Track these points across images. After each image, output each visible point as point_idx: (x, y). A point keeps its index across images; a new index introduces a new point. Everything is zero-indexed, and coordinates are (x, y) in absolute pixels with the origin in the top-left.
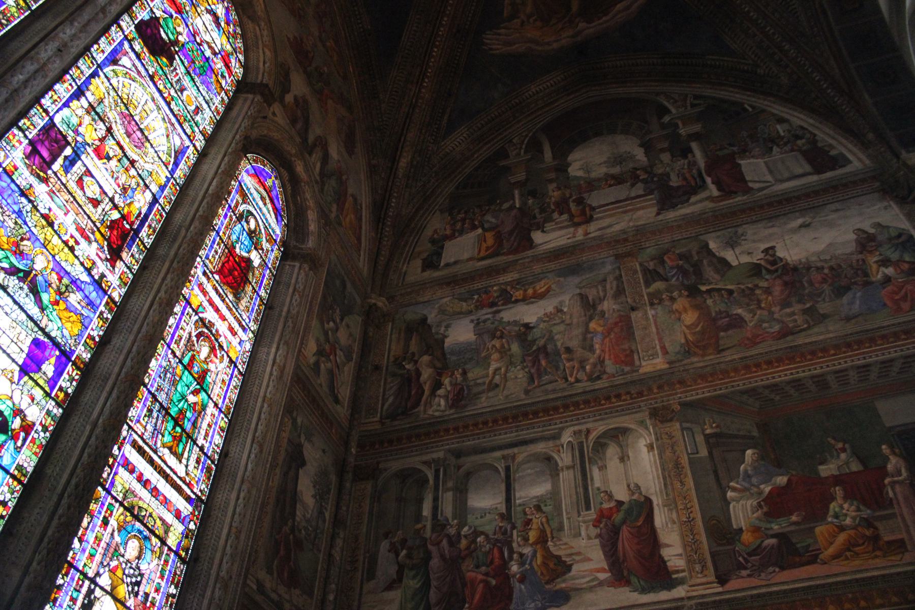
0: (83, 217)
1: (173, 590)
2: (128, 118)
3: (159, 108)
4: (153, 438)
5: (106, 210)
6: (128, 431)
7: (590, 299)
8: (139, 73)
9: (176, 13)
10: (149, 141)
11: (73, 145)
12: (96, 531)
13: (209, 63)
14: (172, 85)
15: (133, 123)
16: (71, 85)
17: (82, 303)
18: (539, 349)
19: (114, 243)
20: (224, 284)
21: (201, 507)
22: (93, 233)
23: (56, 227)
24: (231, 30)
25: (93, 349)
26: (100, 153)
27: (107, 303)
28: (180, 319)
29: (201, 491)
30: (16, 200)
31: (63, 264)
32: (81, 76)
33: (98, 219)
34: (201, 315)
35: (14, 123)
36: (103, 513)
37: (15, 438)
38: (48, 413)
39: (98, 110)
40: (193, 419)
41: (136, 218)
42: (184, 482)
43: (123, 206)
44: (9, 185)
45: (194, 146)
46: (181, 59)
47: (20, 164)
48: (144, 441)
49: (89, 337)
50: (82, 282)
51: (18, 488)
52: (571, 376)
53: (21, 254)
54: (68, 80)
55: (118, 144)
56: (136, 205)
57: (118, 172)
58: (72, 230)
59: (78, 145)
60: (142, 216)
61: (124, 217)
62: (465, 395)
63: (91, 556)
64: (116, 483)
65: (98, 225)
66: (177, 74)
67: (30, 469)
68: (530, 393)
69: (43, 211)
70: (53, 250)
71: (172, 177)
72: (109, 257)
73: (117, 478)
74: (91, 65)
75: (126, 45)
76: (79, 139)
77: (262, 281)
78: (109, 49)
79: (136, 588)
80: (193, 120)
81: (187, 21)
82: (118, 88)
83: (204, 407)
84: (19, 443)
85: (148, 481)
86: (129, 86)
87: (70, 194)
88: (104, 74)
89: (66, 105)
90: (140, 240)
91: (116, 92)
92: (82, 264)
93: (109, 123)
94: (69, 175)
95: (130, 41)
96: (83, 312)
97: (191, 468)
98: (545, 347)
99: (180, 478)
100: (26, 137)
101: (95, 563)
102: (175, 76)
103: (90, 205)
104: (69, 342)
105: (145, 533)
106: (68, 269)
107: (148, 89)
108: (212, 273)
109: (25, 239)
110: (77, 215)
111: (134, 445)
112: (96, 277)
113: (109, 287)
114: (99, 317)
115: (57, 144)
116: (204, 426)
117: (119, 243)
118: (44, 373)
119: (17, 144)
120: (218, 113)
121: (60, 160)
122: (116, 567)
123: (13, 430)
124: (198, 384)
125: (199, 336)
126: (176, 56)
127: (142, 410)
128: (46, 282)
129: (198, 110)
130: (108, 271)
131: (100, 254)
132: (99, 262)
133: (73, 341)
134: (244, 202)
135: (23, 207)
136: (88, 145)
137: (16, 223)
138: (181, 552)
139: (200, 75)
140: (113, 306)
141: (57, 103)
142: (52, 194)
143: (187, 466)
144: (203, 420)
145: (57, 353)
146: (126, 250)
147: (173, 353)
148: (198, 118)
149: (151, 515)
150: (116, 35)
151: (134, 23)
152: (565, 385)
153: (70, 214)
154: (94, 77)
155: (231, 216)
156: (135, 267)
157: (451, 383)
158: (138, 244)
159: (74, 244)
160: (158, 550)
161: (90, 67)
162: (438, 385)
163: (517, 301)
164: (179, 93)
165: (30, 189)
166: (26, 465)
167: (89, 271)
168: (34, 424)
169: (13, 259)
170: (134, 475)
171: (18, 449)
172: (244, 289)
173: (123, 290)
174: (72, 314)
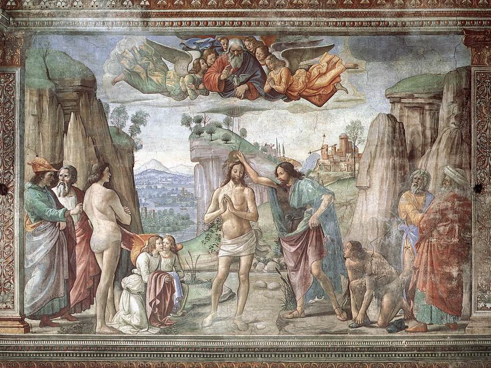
7: (408, 131)
18: (307, 231)
52: (358, 310)
62: (176, 302)
68: (289, 328)
98: (318, 229)
152: (344, 326)
157: (149, 264)
162: (124, 267)
163: (272, 95)
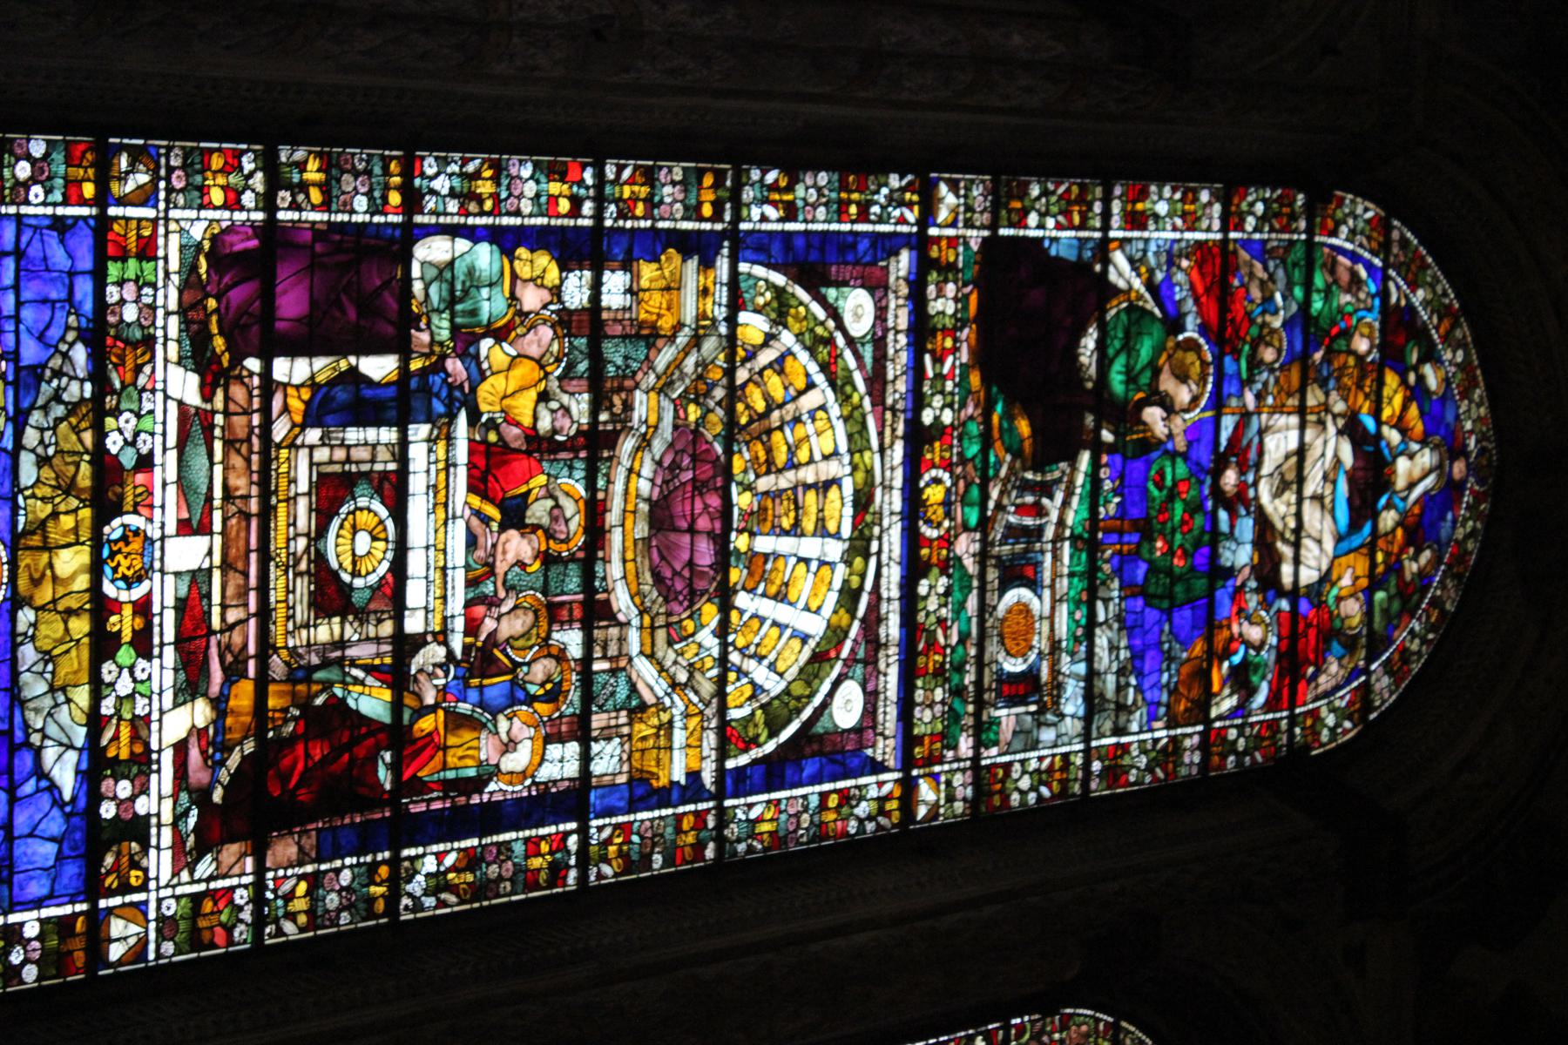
0: (243, 593)
2: (706, 471)
3: (860, 546)
5: (350, 652)
8: (877, 382)
9: (1203, 329)
10: (726, 607)
11: (416, 365)
13: (1212, 590)
14: (984, 524)
15: (715, 501)
19: (284, 778)
22: (234, 672)
23: (114, 529)
24: (1411, 568)
27: (65, 924)
30: (54, 333)
31: (28, 654)
32: (640, 209)
33: (293, 651)
39: (615, 354)
41: (448, 786)
43: (430, 699)
44: (72, 274)
45: (908, 787)
46: (1095, 481)
47: (171, 250)
50: (40, 772)
54: (581, 183)
55: (595, 510)
56: (487, 749)
57: (509, 588)
58: (165, 593)
59: (436, 380)
60: (475, 800)
61: (397, 734)
65: (277, 665)
66: (1039, 511)
69: (114, 443)
70: (36, 582)
72: (217, 796)
74: (707, 210)
75: (903, 263)
76: (455, 366)
80: (980, 704)
81: (1230, 388)
82: (751, 356)
86: (800, 383)
87: (266, 493)
88: (734, 274)
89: (507, 241)
90: (395, 862)
91: (731, 359)
92: (95, 722)
93: (614, 418)
94: (313, 435)
95: (924, 265)
100: (268, 203)
102: (1021, 509)
103: (302, 586)
106: (34, 687)
107: (872, 459)
110: (226, 566)
112: (108, 810)
113: (125, 888)
115: (359, 315)
117: (303, 796)
119: (217, 196)
120: (1114, 773)
121: (322, 366)
126: (1085, 459)
129: (1022, 688)
130: (167, 836)
131: (194, 754)
132: (164, 779)
135: (58, 374)
139: (1130, 589)
140: (80, 958)
141: (473, 207)
142: (196, 429)
146: (310, 842)
148: (1006, 717)
151: (994, 226)
153: (201, 542)
154: (686, 255)
156: (289, 927)
158: (375, 865)
159: (127, 635)
161: (693, 212)
164: (992, 575)
165: (135, 345)
167: (96, 767)
173: (168, 947)
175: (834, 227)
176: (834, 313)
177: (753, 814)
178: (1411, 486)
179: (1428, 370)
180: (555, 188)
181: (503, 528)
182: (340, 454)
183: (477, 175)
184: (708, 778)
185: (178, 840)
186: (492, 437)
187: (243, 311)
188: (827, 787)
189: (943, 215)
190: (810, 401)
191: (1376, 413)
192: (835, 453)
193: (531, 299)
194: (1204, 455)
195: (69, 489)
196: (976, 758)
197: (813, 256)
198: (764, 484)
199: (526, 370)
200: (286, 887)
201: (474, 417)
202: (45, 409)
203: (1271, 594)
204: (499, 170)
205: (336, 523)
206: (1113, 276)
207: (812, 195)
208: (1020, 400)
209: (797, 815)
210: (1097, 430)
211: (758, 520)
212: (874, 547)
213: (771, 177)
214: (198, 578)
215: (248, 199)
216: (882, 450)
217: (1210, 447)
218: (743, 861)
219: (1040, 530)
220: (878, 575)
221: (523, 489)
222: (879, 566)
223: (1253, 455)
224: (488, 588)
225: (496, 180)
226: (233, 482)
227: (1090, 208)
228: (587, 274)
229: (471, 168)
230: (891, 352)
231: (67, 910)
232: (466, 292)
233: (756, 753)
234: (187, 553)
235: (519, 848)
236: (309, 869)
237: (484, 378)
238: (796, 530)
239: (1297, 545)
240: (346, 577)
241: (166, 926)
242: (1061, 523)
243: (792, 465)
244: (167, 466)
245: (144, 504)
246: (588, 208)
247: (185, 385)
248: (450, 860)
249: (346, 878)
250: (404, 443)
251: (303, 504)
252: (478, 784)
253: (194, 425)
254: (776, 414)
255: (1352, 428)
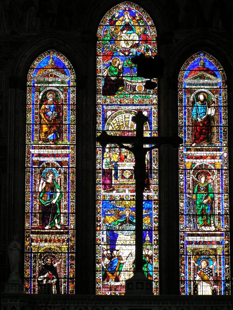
1: (227, 266)
4: (195, 228)
6: (184, 233)
8: (116, 110)
11: (113, 169)
12: (188, 268)
16: (100, 150)
17: (146, 211)
20: (199, 142)
21: (228, 233)
23: (125, 199)
25: (158, 221)
26: (121, 160)
27: (154, 203)
28: (185, 179)
29: (225, 228)
30: (110, 204)
34: (194, 168)
35: (95, 184)
36: (188, 262)
37: (149, 262)
38: (155, 249)
40: (210, 208)
42: (216, 231)
44: (106, 203)
45: (153, 104)
47: (104, 194)
48: (192, 232)
49: (154, 218)
51: (157, 273)
53: (120, 217)
60: (149, 161)
63: (190, 275)
64: (188, 251)
67: (158, 266)
69: (119, 199)
70: (129, 206)
71: (152, 131)
73: (188, 249)
77: (221, 117)
78: (101, 119)
79: (211, 274)
83: (213, 199)
84: (151, 263)
85: (200, 242)
89: (103, 158)
94: (118, 179)
96: (148, 214)
97: (217, 224)
99: (214, 231)
101: (192, 276)
103: (130, 180)
104: (149, 226)
105: (207, 257)
108: (191, 146)
109: (120, 212)
110: (128, 188)
111: (189, 235)
112: (146, 199)
113: (152, 197)
114: (154, 210)
116: (216, 205)
118: (147, 241)
119: (100, 189)
121: (113, 178)
122: (200, 273)
123: (147, 261)
124: (206, 194)
125: (197, 177)
126: (124, 78)
127: (186, 223)
128: (132, 217)
130: (149, 193)
133: (150, 225)
134: (191, 94)
136: (117, 162)
137: (114, 210)
138: (226, 253)
140: (157, 201)
143: (215, 225)
144: (214, 204)
145: (148, 232)
147: (189, 194)
149: (206, 251)
150: (99, 109)
153: (126, 190)
155: (188, 110)
159: (133, 197)
160: (215, 258)
166: (156, 266)
168: (152, 255)
169: (120, 220)
170: (193, 244)
171: (152, 264)
172: (211, 133)
174: (145, 218)
175: (101, 117)
176: (109, 116)
177: (154, 126)
178: (129, 19)
179: (116, 16)
180: (99, 153)
181: (127, 158)
182: (120, 176)
183: (98, 162)
184: (150, 132)
185: (149, 192)
186: (119, 160)
187: (109, 186)
188: (152, 116)
189: (100, 102)
190: (117, 120)
191: (121, 26)
192: (122, 116)
193: (108, 156)
194: (124, 58)
195: (122, 203)
196: (152, 94)
197: (104, 120)
198: (124, 126)
199: (114, 156)
200: (154, 181)
201: (117, 162)
202: (116, 205)
203: (139, 45)
204: (97, 160)
205: (125, 177)
206: (105, 75)
207: (99, 120)
208: (117, 90)
209: (155, 120)
210: (121, 76)
211: (127, 126)
212: (131, 110)
213: (97, 126)
214: (129, 191)
215: (100, 186)
216: (122, 110)
217: (123, 57)
218: (158, 127)
219: (131, 85)
220: (134, 110)
221: (124, 156)
222: (132, 109)
223: (124, 49)
224: (132, 160)
225: (98, 160)
226: (122, 187)
227: (99, 79)
228: (106, 149)
229: (97, 163)
230: (113, 109)
231: (153, 203)
232: (107, 163)
233: (148, 126)
234: (127, 191)
235: (154, 156)
236: (153, 179)
237: (114, 161)
238: (128, 121)
239: (134, 40)
240: (130, 175)
241: (156, 193)
242: (130, 82)
243: (123, 122)
244: (121, 194)
245: (123, 196)
246: (100, 149)
247: (114, 192)
248: (154, 164)
249: (154, 175)
250: (119, 170)
251: (124, 180)
252: (148, 160)
253: (118, 191)
254: (118, 124)
255: (122, 31)
